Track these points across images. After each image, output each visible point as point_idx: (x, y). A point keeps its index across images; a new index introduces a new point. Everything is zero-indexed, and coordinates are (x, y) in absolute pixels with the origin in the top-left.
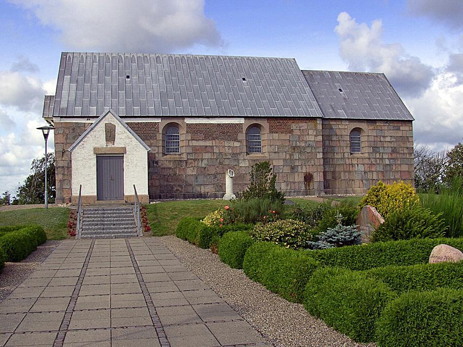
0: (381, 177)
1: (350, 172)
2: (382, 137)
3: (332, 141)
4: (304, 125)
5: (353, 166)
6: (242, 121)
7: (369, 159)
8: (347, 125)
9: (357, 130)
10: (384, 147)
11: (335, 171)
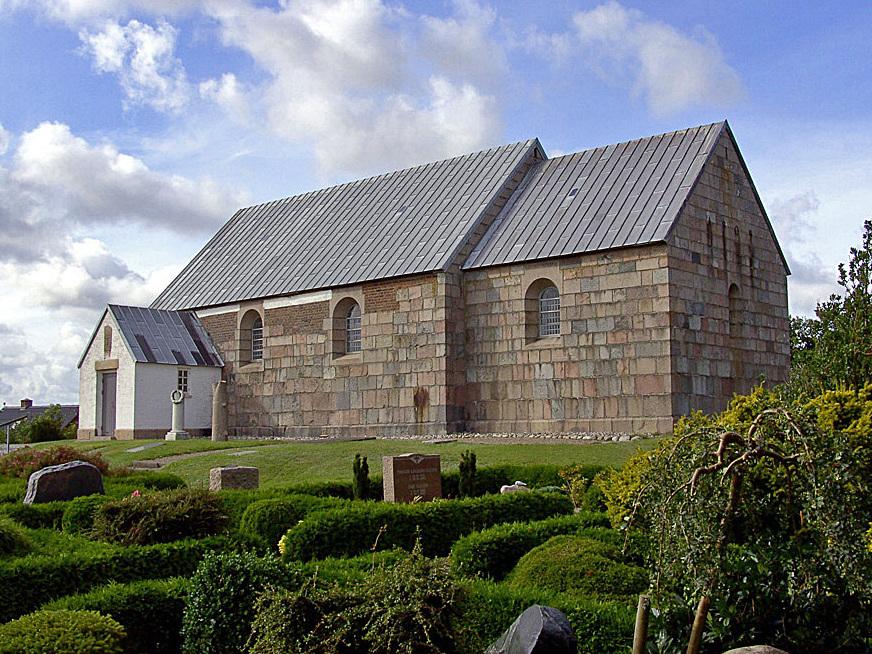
0: (589, 392)
1: (525, 382)
2: (592, 295)
3: (491, 314)
4: (415, 291)
5: (530, 370)
6: (328, 296)
7: (564, 349)
8: (520, 276)
9: (542, 286)
10: (597, 319)
11: (496, 382)
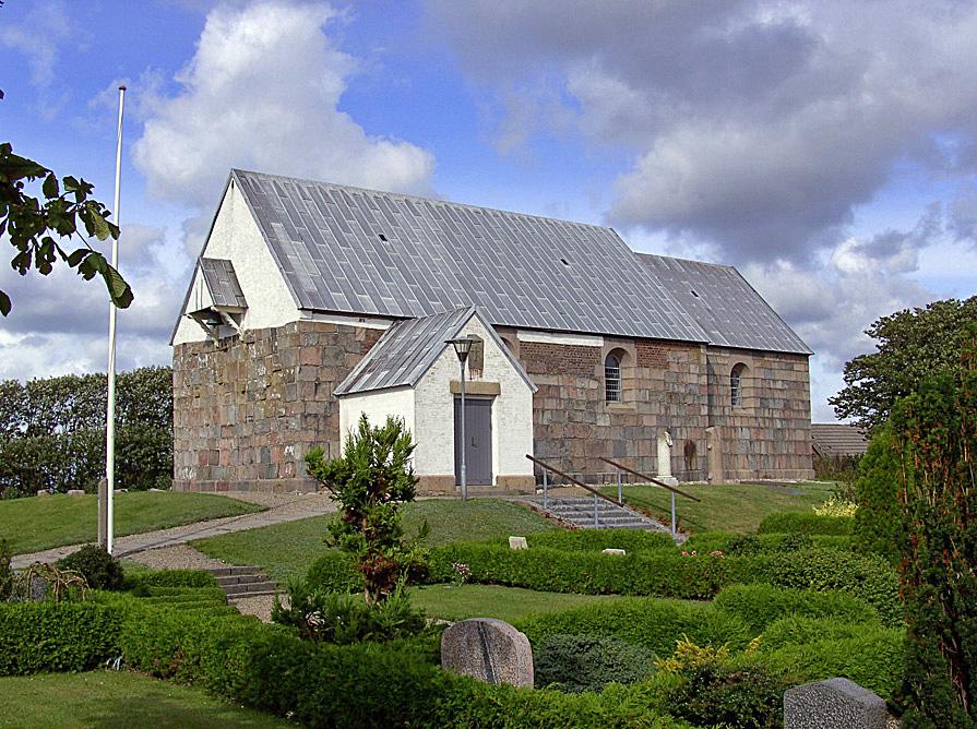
0: (771, 451)
1: (732, 441)
4: (683, 355)
6: (600, 342)
